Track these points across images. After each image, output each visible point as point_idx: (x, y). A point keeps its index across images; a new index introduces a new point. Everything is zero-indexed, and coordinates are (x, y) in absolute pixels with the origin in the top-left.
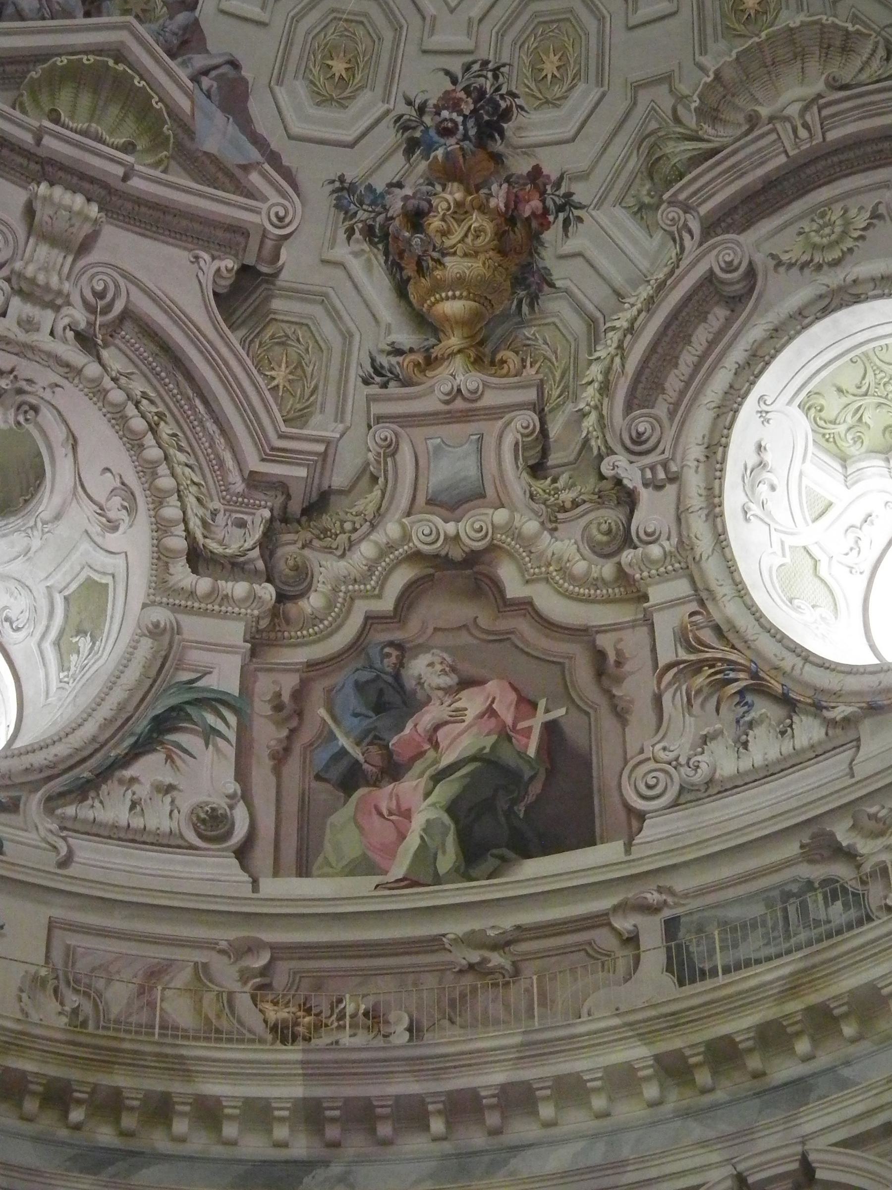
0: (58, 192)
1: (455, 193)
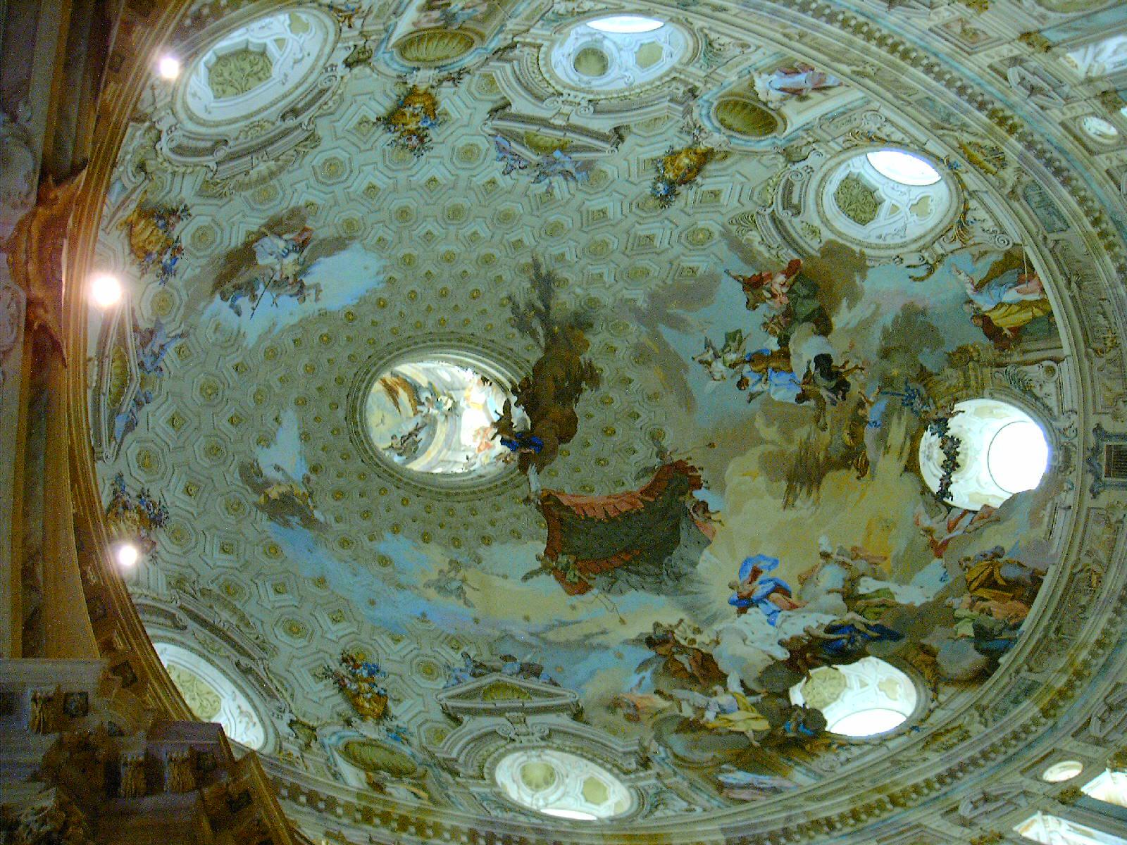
0: (96, 369)
1: (137, 517)
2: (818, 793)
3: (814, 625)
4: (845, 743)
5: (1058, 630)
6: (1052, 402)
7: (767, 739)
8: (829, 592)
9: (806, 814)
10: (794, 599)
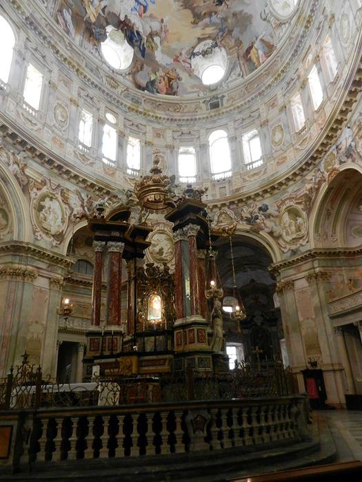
2: (74, 47)
3: (137, 26)
4: (98, 50)
5: (160, 105)
6: (230, 79)
7: (88, 23)
8: (151, 27)
9: (56, 43)
10: (143, 15)
